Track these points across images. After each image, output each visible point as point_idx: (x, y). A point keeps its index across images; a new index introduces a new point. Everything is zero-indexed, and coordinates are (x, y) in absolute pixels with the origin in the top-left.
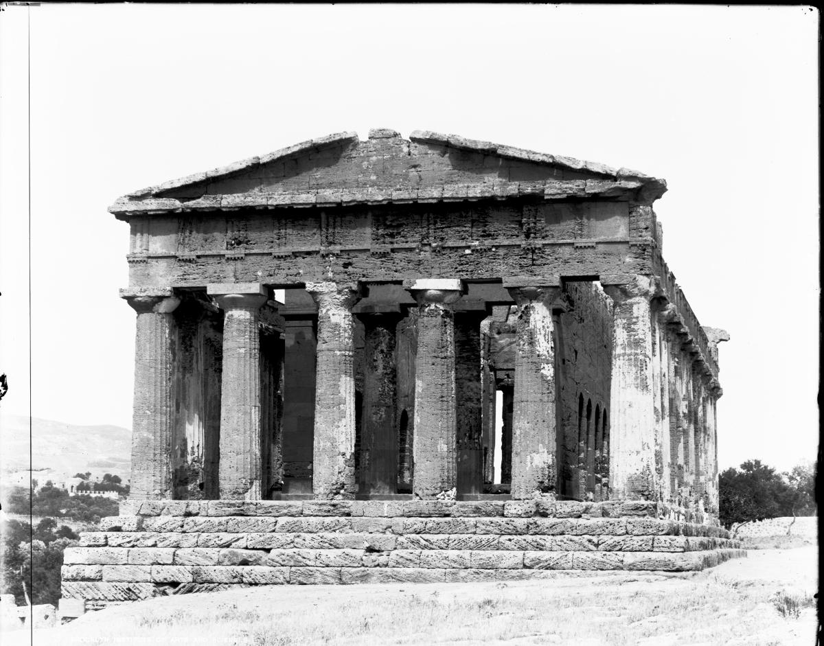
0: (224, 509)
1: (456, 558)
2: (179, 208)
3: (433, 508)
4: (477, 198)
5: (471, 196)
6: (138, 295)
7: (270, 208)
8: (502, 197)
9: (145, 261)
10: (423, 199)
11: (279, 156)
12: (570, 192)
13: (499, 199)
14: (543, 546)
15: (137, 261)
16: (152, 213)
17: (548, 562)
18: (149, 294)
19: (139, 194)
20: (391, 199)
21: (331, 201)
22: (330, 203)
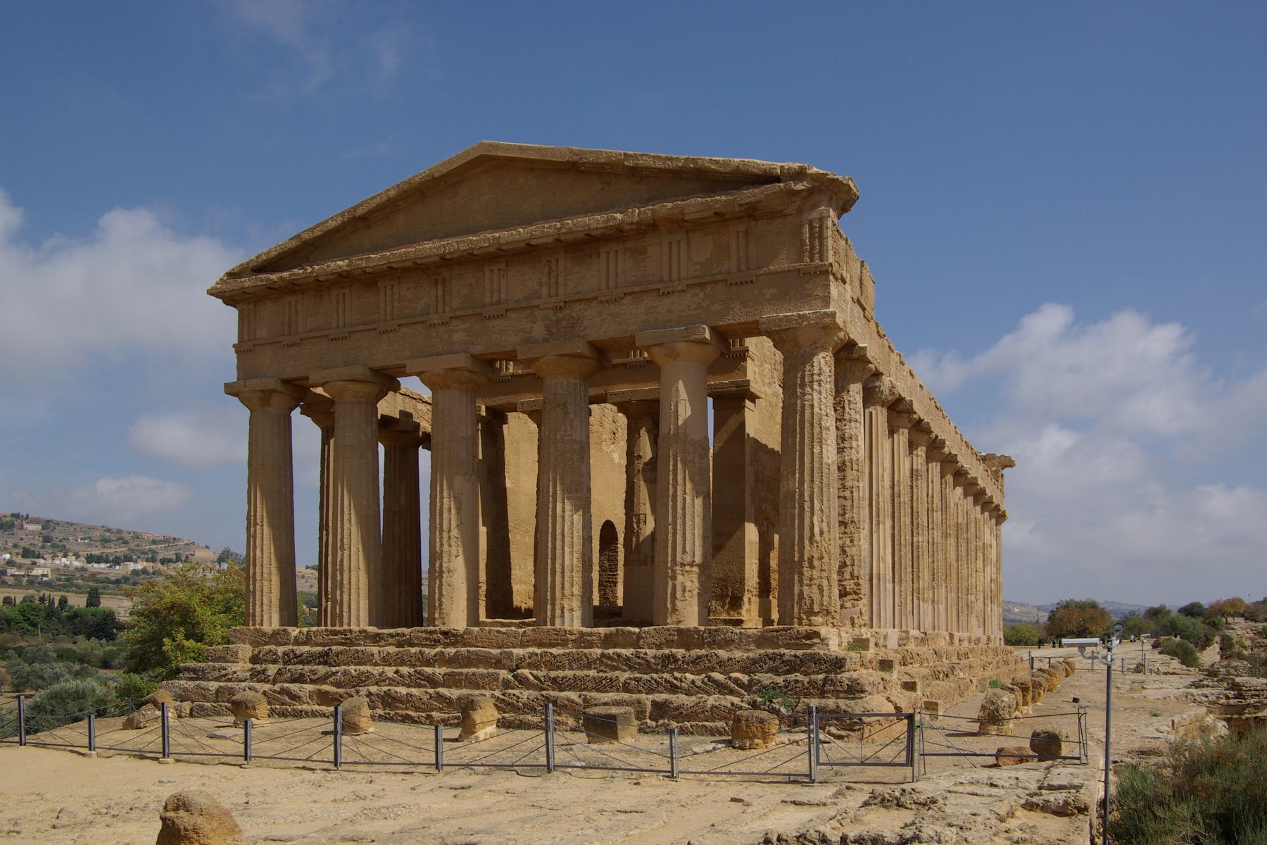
0: (331, 637)
1: (566, 702)
14: (678, 688)
17: (681, 710)
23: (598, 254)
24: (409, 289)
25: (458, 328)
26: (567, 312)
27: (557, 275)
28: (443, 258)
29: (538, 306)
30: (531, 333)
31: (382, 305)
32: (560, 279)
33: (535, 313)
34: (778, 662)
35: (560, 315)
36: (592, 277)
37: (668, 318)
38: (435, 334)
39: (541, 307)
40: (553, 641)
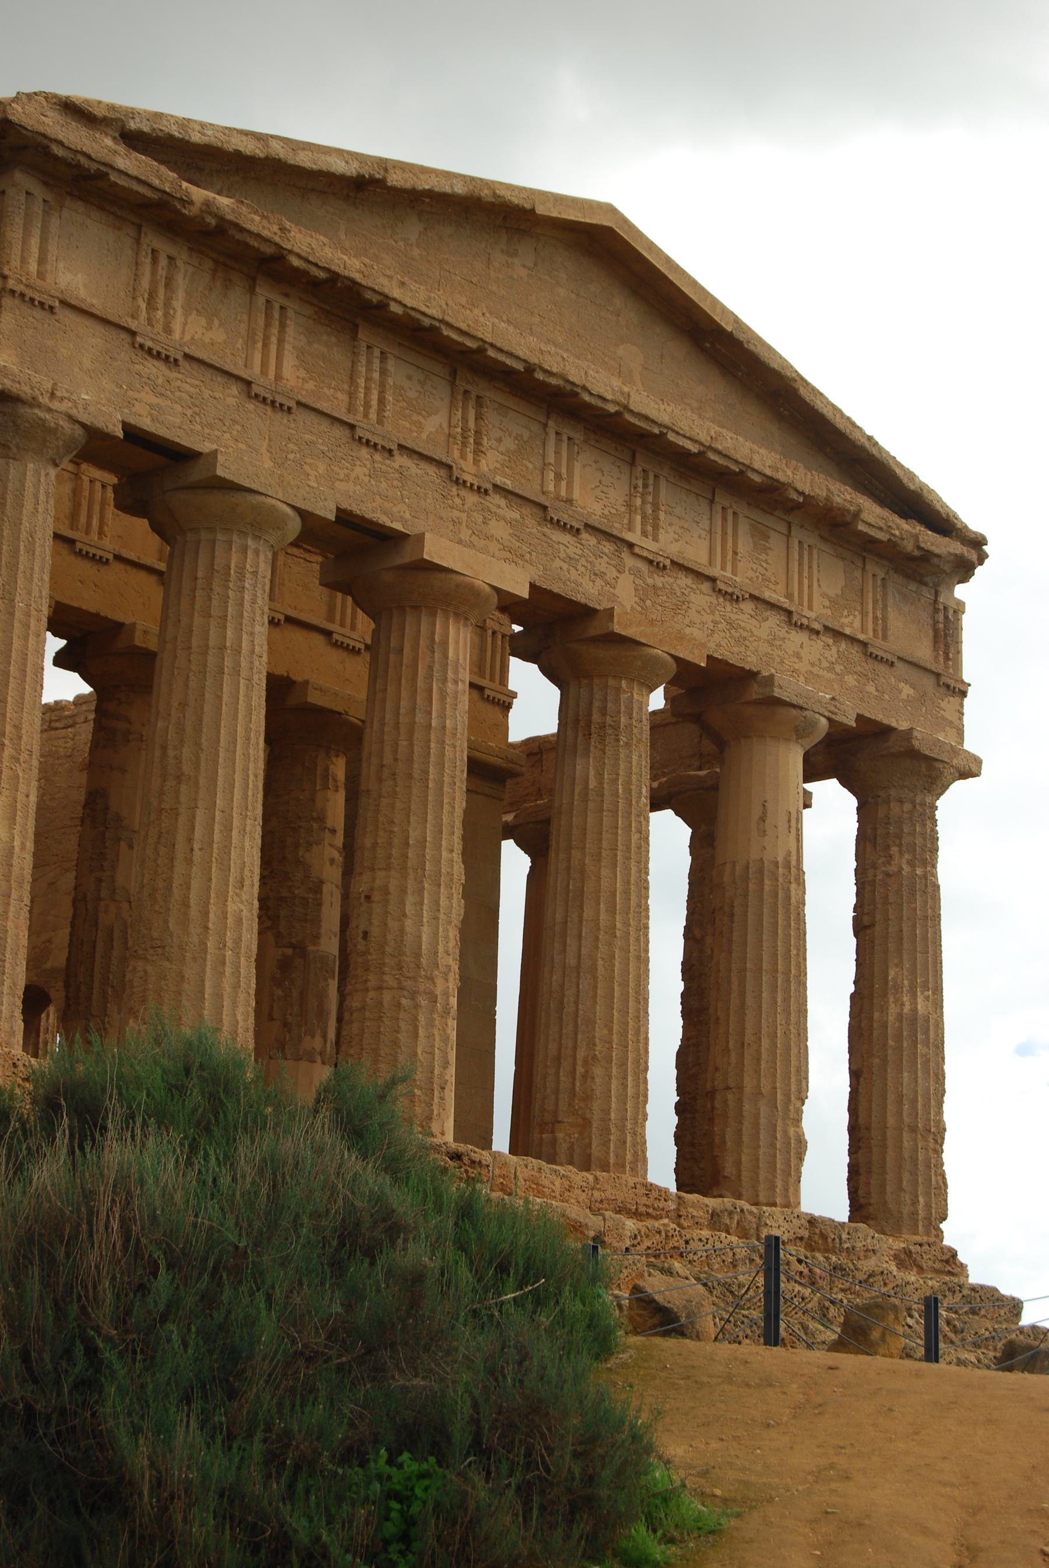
2: (191, 203)
3: (644, 1200)
4: (764, 475)
5: (756, 465)
6: (45, 400)
7: (395, 308)
8: (802, 494)
9: (51, 308)
10: (678, 433)
11: (427, 187)
12: (897, 533)
13: (794, 496)
15: (32, 300)
16: (122, 182)
18: (74, 412)
19: (99, 112)
20: (626, 408)
21: (521, 354)
22: (517, 358)
23: (712, 502)
24: (409, 378)
25: (500, 511)
26: (667, 579)
27: (656, 507)
28: (530, 369)
29: (631, 546)
30: (614, 588)
31: (362, 382)
32: (662, 515)
33: (623, 555)
34: (958, 1296)
35: (659, 580)
36: (700, 537)
37: (797, 666)
38: (458, 501)
39: (637, 550)
40: (642, 1209)
